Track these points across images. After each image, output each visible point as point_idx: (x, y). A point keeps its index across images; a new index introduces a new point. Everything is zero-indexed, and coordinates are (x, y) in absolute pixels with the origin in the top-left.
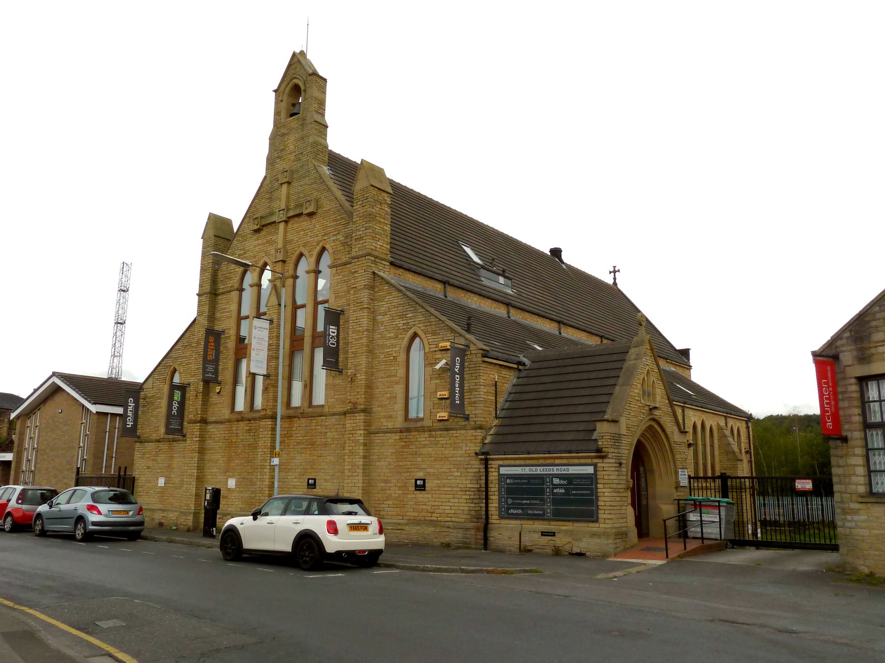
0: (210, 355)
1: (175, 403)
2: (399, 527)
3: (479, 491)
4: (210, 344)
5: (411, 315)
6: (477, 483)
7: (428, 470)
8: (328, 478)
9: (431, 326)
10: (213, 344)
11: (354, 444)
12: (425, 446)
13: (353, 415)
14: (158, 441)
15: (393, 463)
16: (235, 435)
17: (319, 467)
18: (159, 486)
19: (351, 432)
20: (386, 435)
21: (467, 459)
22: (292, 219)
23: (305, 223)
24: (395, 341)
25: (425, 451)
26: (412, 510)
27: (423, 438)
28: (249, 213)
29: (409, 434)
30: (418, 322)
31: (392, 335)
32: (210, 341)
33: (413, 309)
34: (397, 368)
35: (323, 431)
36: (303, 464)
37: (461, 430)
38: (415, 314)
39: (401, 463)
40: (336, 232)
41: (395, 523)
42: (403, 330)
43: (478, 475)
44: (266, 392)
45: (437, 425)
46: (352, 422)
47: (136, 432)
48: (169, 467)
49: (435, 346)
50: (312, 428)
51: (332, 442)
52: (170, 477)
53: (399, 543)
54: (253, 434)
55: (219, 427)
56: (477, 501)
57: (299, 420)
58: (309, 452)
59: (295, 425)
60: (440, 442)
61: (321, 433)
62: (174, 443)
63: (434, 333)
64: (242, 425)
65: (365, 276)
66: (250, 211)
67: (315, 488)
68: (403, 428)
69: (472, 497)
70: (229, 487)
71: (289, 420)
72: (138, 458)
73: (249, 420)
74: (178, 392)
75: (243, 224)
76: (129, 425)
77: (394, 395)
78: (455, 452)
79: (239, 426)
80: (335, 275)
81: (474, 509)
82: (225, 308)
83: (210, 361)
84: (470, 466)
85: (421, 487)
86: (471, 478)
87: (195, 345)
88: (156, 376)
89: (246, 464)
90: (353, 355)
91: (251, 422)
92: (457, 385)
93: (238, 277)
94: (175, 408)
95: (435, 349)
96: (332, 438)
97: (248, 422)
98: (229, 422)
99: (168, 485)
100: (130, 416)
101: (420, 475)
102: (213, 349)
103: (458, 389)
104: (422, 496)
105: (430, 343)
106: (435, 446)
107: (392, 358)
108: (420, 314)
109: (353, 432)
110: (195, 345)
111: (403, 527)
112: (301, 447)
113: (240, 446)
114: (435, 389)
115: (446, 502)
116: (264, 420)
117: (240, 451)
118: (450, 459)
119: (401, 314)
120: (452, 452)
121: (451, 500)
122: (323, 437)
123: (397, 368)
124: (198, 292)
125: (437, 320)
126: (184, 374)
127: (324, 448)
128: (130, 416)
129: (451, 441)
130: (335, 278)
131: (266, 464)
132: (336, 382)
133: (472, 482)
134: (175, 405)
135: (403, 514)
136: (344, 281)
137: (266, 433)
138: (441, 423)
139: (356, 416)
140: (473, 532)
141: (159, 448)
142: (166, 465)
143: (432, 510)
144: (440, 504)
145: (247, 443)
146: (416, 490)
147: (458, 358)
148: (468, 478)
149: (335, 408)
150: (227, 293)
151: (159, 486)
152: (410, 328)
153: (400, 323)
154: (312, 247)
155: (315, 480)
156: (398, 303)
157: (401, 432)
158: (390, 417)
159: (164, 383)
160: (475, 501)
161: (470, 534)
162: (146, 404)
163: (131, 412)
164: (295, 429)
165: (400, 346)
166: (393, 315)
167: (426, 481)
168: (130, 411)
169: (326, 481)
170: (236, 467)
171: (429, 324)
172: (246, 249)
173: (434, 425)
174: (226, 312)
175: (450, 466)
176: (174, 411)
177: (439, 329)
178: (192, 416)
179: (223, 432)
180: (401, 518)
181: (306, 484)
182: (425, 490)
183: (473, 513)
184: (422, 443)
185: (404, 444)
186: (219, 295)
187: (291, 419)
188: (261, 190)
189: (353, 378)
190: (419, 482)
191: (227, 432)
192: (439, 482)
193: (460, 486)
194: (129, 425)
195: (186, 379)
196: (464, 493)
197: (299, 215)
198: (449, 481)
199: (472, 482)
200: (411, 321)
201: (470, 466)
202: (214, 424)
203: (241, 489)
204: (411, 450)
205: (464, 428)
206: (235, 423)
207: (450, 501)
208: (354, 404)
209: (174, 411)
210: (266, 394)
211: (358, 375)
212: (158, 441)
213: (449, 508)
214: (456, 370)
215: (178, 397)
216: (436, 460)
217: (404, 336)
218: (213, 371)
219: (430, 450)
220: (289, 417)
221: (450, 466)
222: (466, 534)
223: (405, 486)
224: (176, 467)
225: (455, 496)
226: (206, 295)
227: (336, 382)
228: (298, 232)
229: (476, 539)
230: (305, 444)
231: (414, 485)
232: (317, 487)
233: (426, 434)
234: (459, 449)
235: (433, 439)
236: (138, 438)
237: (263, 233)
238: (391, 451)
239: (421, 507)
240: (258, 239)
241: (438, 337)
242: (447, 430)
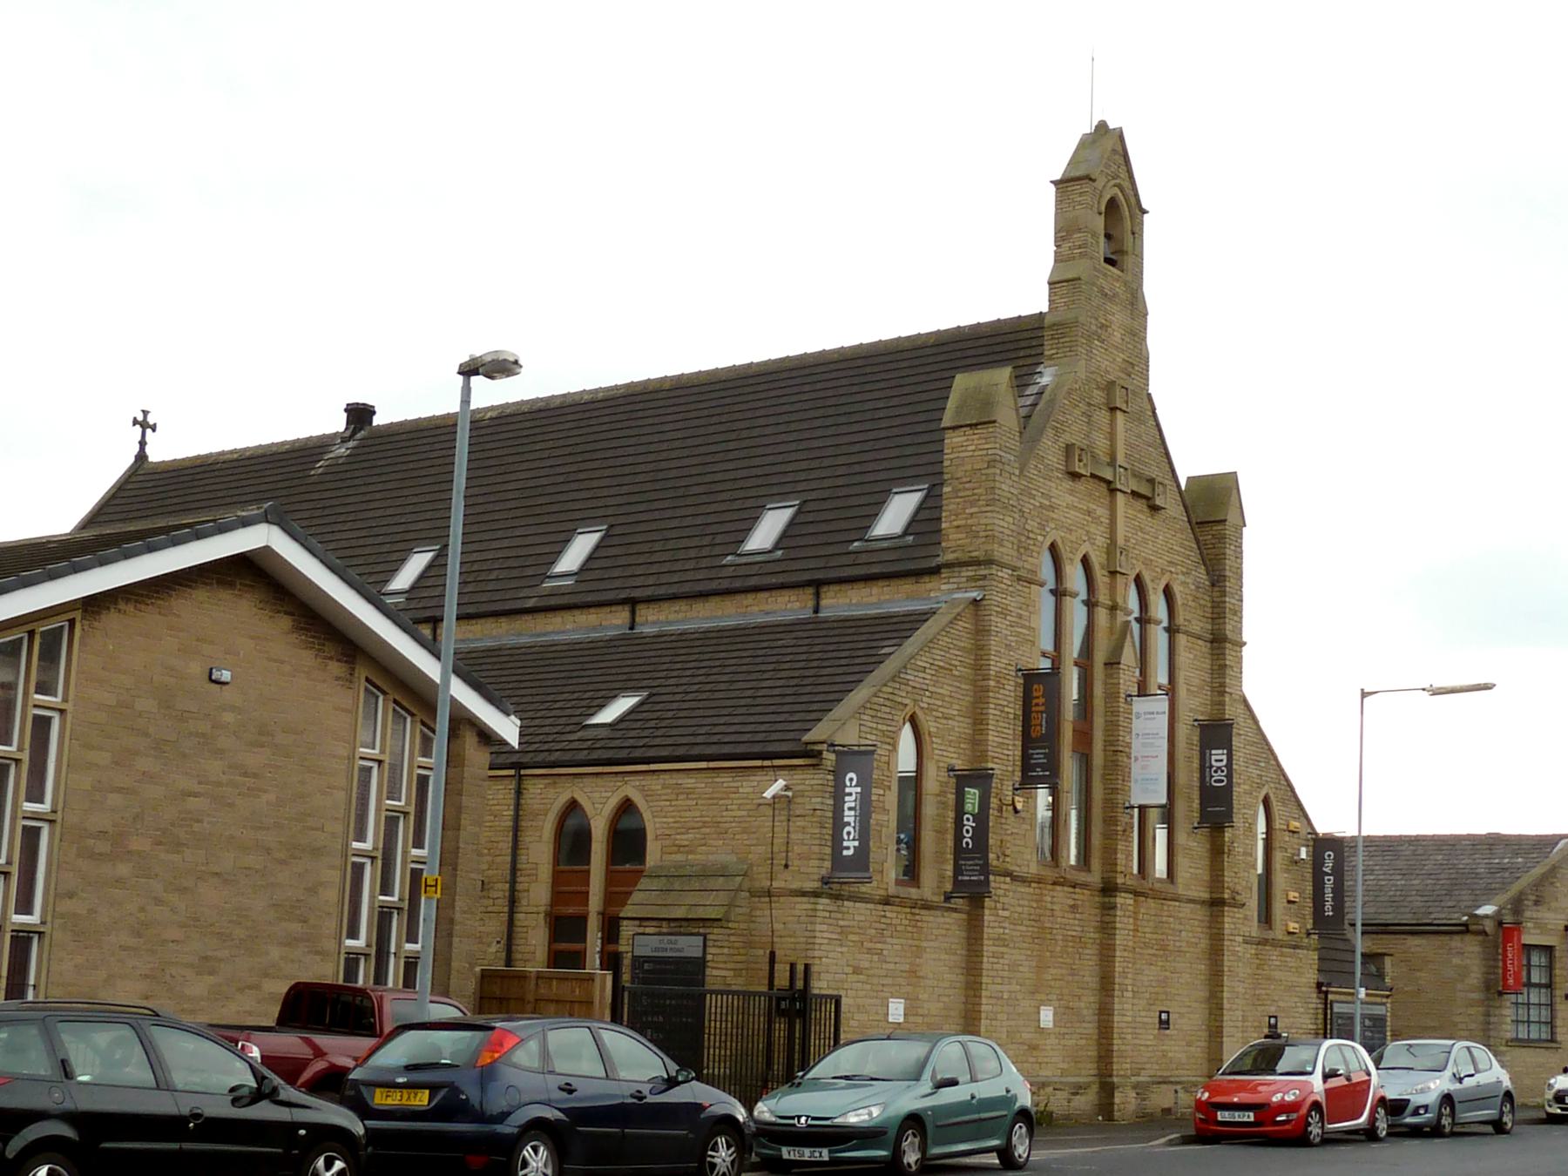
0: (1035, 725)
1: (968, 820)
4: (1035, 701)
10: (1042, 700)
16: (1048, 913)
32: (1035, 694)
55: (1019, 889)
74: (972, 790)
83: (1037, 740)
89: (1070, 978)
91: (1077, 890)
94: (968, 831)
97: (1071, 890)
98: (1039, 883)
100: (849, 824)
102: (1042, 712)
113: (1057, 937)
116: (1123, 894)
117: (1058, 949)
124: (1244, 649)
126: (939, 741)
131: (1127, 982)
134: (969, 824)
137: (1126, 920)
145: (1069, 933)
163: (852, 813)
176: (967, 840)
179: (1026, 903)
191: (1035, 905)
195: (945, 753)
203: (1063, 1030)
206: (1050, 887)
209: (967, 840)
215: (973, 804)
218: (1045, 761)
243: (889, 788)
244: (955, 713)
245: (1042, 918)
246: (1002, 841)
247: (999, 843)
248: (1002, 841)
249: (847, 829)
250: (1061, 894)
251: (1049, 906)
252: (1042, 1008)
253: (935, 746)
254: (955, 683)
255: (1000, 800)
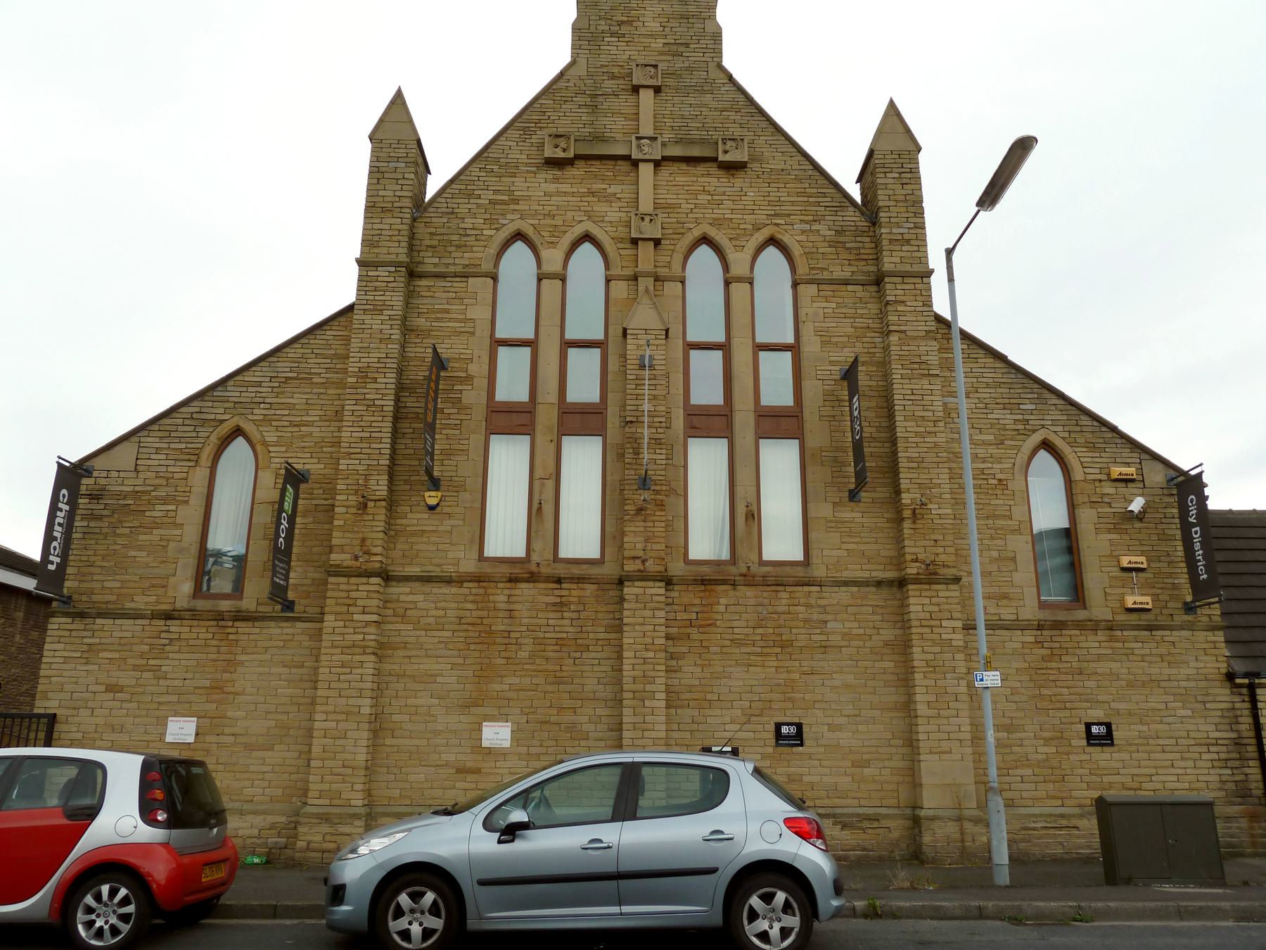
2: (1064, 822)
3: (1236, 744)
5: (1034, 407)
6: (1232, 730)
7: (1113, 705)
8: (843, 720)
9: (1084, 434)
11: (938, 649)
12: (1099, 658)
13: (927, 587)
14: (168, 616)
15: (1023, 691)
17: (808, 697)
18: (169, 739)
19: (924, 623)
20: (997, 632)
21: (1203, 684)
22: (671, 163)
23: (714, 180)
24: (997, 451)
25: (1103, 667)
26: (1084, 785)
27: (1093, 643)
28: (520, 120)
29: (1058, 632)
30: (1050, 423)
31: (992, 437)
33: (1036, 396)
34: (1011, 503)
35: (815, 617)
36: (760, 689)
37: (1184, 629)
38: (1039, 407)
39: (1044, 691)
40: (811, 218)
41: (1051, 815)
42: (1016, 433)
43: (1231, 714)
44: (640, 518)
45: (1123, 617)
46: (927, 601)
47: (62, 587)
48: (217, 687)
49: (1097, 471)
50: (780, 609)
51: (846, 643)
52: (224, 717)
53: (1066, 856)
54: (575, 615)
55: (436, 590)
56: (1237, 763)
57: (735, 589)
58: (774, 664)
59: (723, 601)
60: (1137, 652)
61: (806, 621)
62: (237, 624)
63: (1092, 447)
64: (525, 589)
65: (925, 314)
66: (525, 117)
67: (801, 745)
68: (1045, 621)
69: (1223, 756)
70: (485, 744)
71: (702, 588)
72: (61, 660)
73: (559, 581)
75: (501, 138)
76: (52, 563)
77: (1012, 555)
78: (1174, 671)
79: (513, 592)
80: (814, 299)
81: (1229, 778)
82: (447, 311)
84: (1211, 698)
85: (1101, 737)
86: (1218, 720)
87: (354, 380)
88: (151, 441)
89: (550, 688)
90: (915, 465)
91: (564, 586)
92: (1197, 546)
93: (493, 250)
95: (1099, 477)
96: (844, 634)
99: (214, 739)
101: (1097, 714)
103: (1201, 552)
104: (1107, 756)
105: (1086, 465)
106: (1125, 657)
107: (995, 482)
108: (1053, 408)
109: (933, 623)
110: (354, 380)
111: (1074, 822)
112: (744, 650)
114: (1109, 552)
115: (1165, 767)
117: (523, 654)
118: (1163, 684)
119: (1007, 401)
120: (1167, 671)
121: (1176, 764)
122: (818, 631)
123: (1011, 503)
125: (1095, 423)
127: (821, 656)
128: (56, 539)
129: (1163, 651)
130: (815, 305)
132: (843, 515)
133: (1220, 727)
135: (1064, 795)
136: (843, 316)
138: (1135, 616)
139: (937, 591)
140: (1244, 823)
141: (163, 635)
142: (207, 683)
143: (1135, 785)
144: (1154, 771)
146: (1089, 744)
147: (1192, 497)
148: (1209, 720)
149: (847, 569)
150: (456, 276)
151: (169, 739)
152: (1034, 431)
153: (1008, 418)
154: (738, 232)
155: (799, 726)
156: (996, 380)
157: (1040, 627)
158: (1005, 596)
159: (192, 464)
160: (1230, 764)
161: (1238, 828)
162: (106, 512)
164: (722, 608)
165: (1013, 461)
166: (985, 401)
167: (1114, 727)
168: (60, 524)
169: (833, 728)
170: (511, 695)
171: (1078, 429)
172: (516, 193)
173: (1118, 618)
174: (450, 320)
175: (1166, 699)
177: (1102, 441)
178: (348, 556)
179: (454, 605)
180: (1060, 802)
181: (771, 735)
182: (1112, 744)
183: (1232, 786)
184: (1093, 651)
185: (1049, 652)
186: (421, 276)
187: (709, 587)
188: (562, 84)
189: (917, 511)
190: (1095, 729)
192: (1145, 728)
193: (1192, 735)
194: (52, 563)
196: (1205, 749)
197: (715, 160)
198: (1167, 727)
199: (1220, 727)
200: (1032, 417)
201: (1211, 698)
202: (417, 584)
204: (1069, 665)
205: (1190, 627)
207: (1175, 766)
208: (929, 565)
210: (642, 524)
211: (930, 506)
212: (168, 616)
213: (1175, 778)
214: (1191, 520)
216: (1130, 685)
217: (1021, 443)
219: (1115, 666)
220: (703, 580)
221: (1166, 699)
222: (1231, 828)
223: (1062, 738)
224: (249, 690)
225: (1186, 755)
226: (393, 269)
227: (843, 515)
228: (696, 194)
229: (1253, 836)
230: (762, 644)
231: (1084, 735)
232: (806, 742)
233: (1102, 635)
234: (1182, 665)
235: (1120, 645)
236: (64, 603)
237: (571, 172)
238: (1015, 665)
239: (1106, 779)
240: (556, 180)
241: (1103, 455)
242: (1150, 628)
243: (186, 502)
244: (317, 418)
245: (485, 621)
246: (363, 540)
247: (359, 542)
248: (363, 540)
249: (55, 544)
250: (532, 592)
251: (502, 606)
252: (484, 724)
253: (272, 455)
254: (315, 391)
255: (363, 497)
